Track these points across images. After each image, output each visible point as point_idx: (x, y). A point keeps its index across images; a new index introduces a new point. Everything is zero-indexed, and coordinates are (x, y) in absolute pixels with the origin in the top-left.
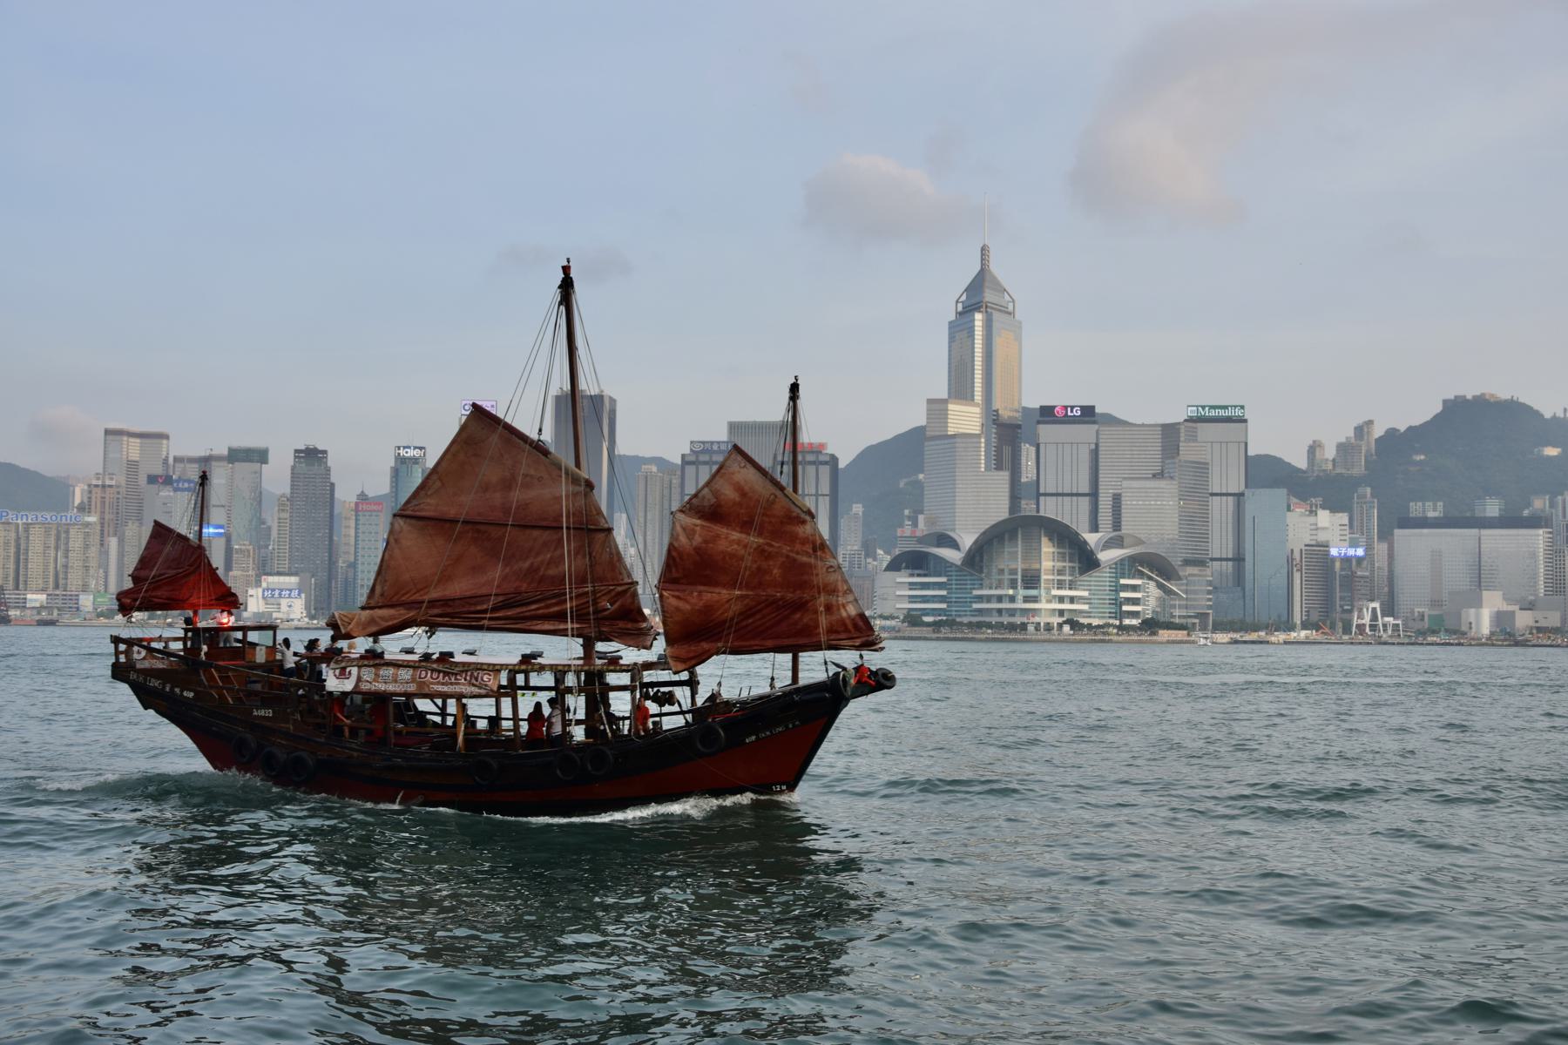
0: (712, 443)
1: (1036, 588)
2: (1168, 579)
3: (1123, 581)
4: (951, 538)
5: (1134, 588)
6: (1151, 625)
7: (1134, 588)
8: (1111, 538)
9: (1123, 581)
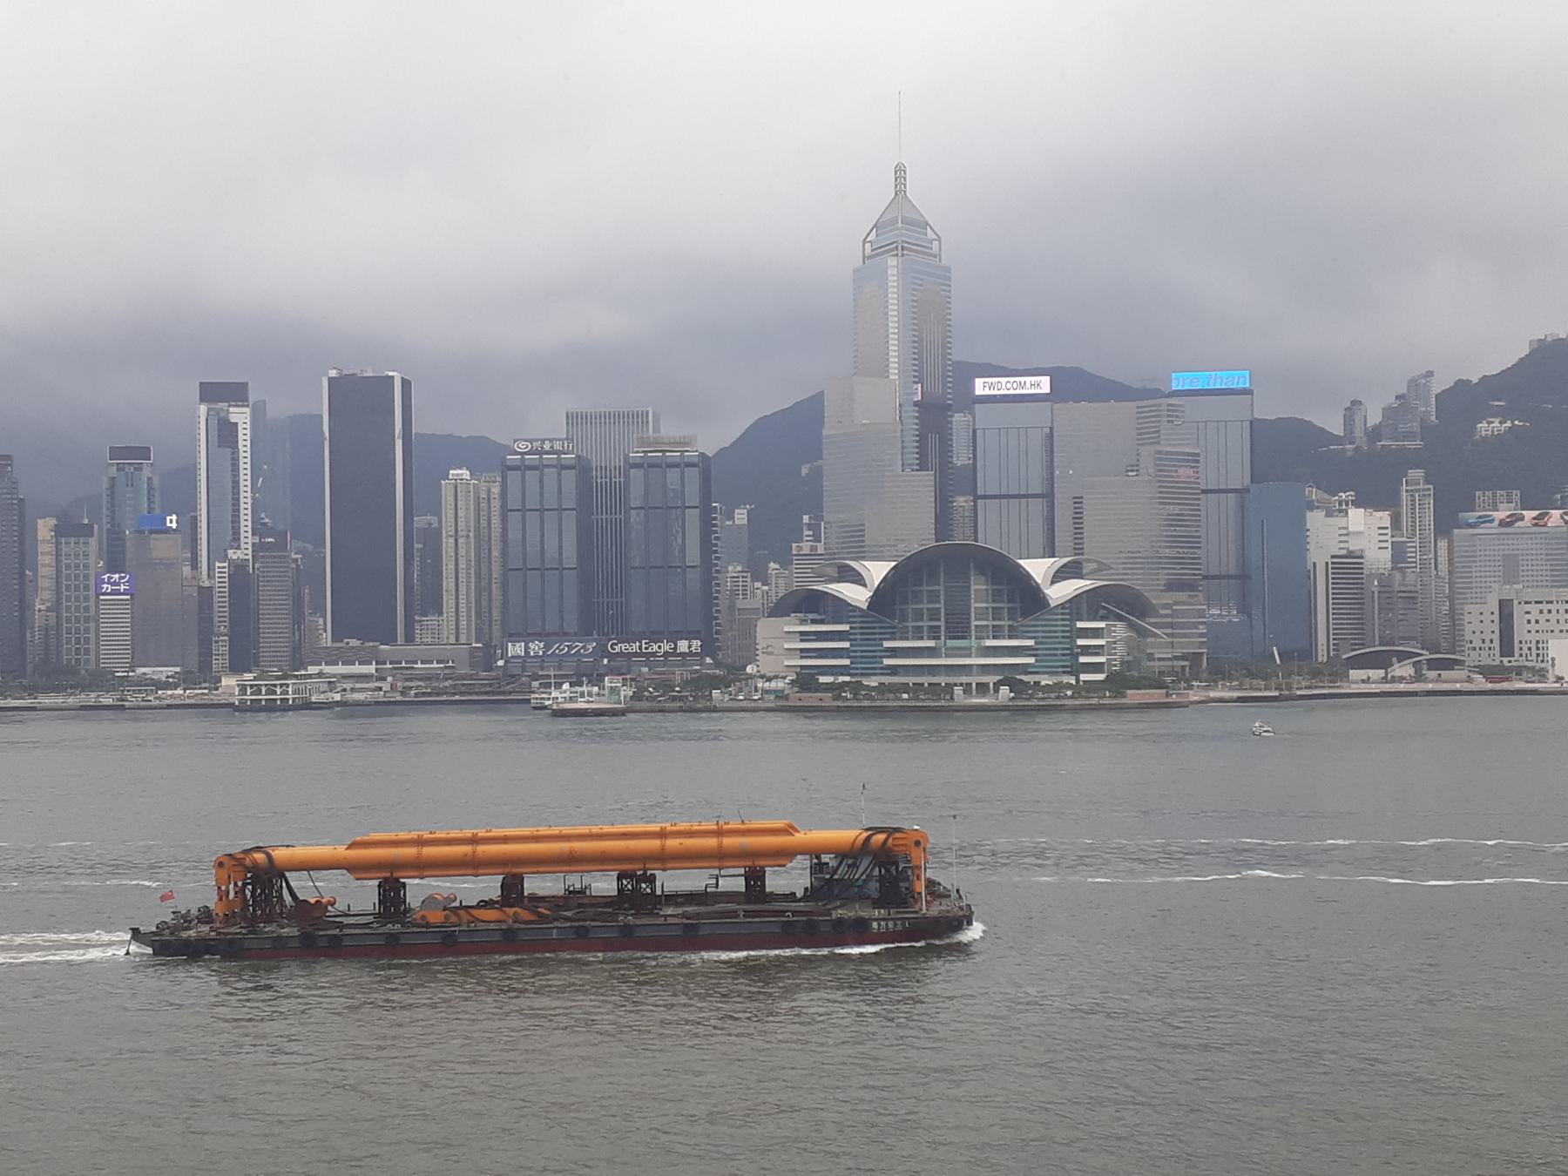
0: (543, 441)
1: (963, 638)
2: (1142, 616)
3: (1080, 625)
4: (857, 571)
5: (1096, 633)
6: (1118, 682)
7: (1096, 633)
8: (1062, 567)
9: (1080, 625)
